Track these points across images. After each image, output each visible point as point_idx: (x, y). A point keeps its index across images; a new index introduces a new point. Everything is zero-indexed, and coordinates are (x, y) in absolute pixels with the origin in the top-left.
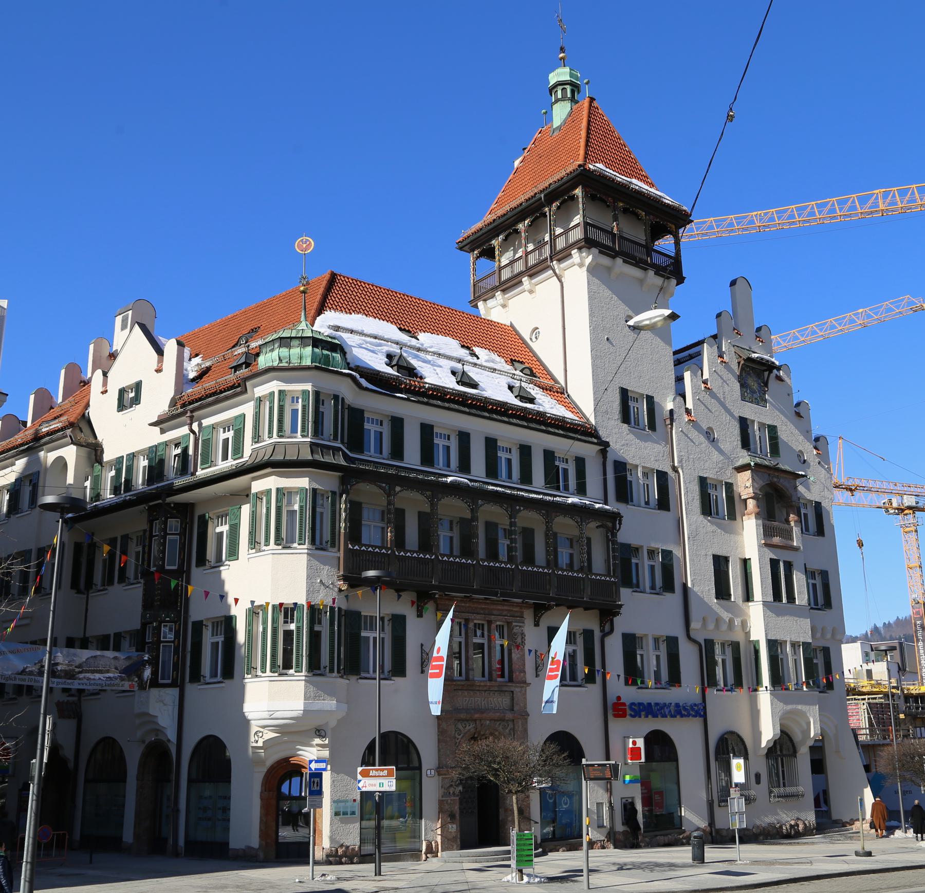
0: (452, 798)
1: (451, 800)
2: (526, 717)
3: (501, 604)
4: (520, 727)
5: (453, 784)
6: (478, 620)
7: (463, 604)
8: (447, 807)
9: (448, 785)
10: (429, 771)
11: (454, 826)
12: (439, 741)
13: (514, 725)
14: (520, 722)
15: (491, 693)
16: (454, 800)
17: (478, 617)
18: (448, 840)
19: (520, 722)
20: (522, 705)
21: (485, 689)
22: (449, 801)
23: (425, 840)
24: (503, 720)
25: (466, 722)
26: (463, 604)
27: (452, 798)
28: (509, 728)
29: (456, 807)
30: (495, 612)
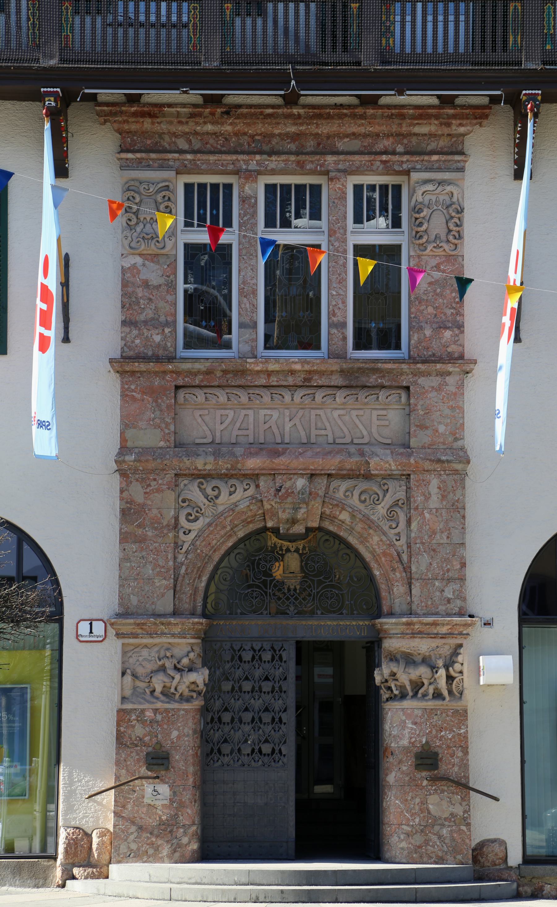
0: (159, 705)
1: (156, 711)
2: (459, 467)
3: (354, 116)
4: (434, 498)
5: (169, 664)
6: (273, 172)
7: (209, 127)
8: (139, 731)
9: (150, 667)
10: (84, 628)
11: (164, 789)
12: (124, 538)
13: (408, 488)
14: (435, 483)
15: (319, 395)
16: (167, 711)
17: (274, 162)
18: (141, 828)
19: (435, 483)
20: (442, 429)
21: (290, 380)
22: (149, 714)
23: (67, 827)
24: (368, 477)
25: (220, 484)
26: (209, 127)
27: (159, 705)
28: (388, 500)
29: (175, 734)
30: (341, 145)
